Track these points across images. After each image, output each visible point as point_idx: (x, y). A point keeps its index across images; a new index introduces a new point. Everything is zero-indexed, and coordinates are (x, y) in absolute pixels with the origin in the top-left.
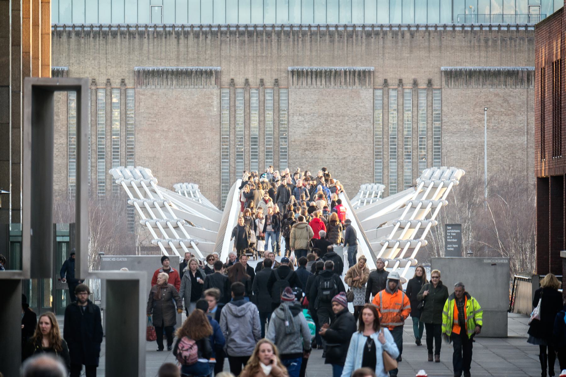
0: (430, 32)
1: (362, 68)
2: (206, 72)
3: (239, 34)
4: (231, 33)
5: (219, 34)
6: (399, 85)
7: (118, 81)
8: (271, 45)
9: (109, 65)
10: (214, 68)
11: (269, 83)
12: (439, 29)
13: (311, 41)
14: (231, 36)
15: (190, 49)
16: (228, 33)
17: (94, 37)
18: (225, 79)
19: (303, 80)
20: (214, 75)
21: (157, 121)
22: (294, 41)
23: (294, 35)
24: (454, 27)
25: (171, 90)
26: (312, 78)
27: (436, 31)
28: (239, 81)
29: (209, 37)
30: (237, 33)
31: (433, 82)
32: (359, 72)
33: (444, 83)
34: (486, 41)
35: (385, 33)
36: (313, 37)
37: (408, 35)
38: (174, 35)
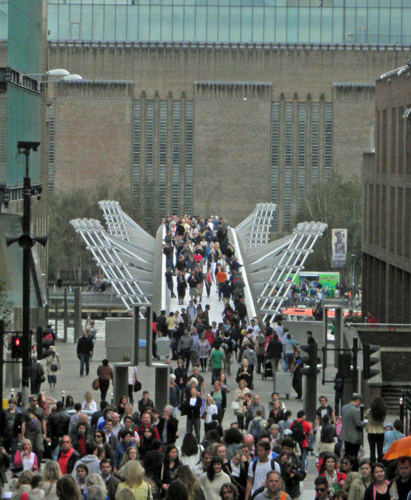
0: (323, 51)
1: (261, 83)
2: (120, 85)
4: (143, 49)
5: (132, 50)
6: (294, 99)
8: (179, 61)
10: (127, 82)
11: (177, 96)
12: (331, 48)
13: (215, 58)
18: (137, 92)
19: (208, 94)
20: (127, 88)
22: (200, 55)
23: (200, 51)
24: (345, 46)
25: (88, 100)
26: (215, 91)
27: (328, 50)
28: (150, 94)
29: (123, 52)
30: (149, 50)
31: (325, 96)
32: (259, 87)
33: (335, 97)
34: (374, 60)
35: (282, 51)
36: (217, 54)
37: (303, 54)
38: (91, 51)
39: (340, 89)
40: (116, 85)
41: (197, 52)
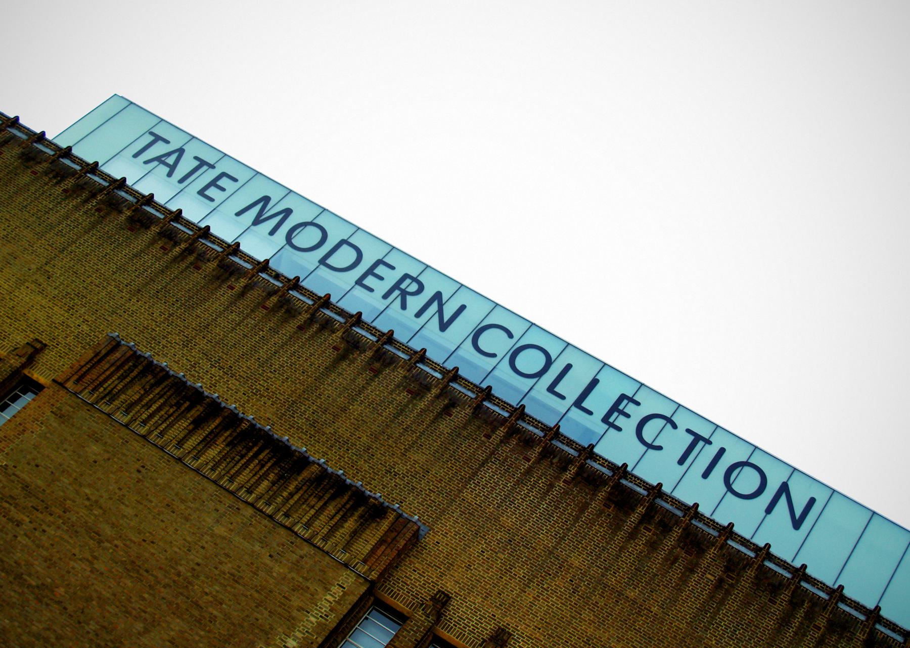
3: (577, 474)
5: (501, 432)
8: (684, 580)
9: (35, 282)
14: (545, 463)
15: (356, 409)
16: (538, 449)
20: (385, 525)
21: (27, 526)
22: (784, 621)
25: (178, 467)
30: (573, 470)
41: (785, 596)
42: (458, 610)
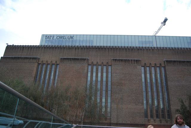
2: (84, 59)
4: (93, 48)
7: (55, 61)
13: (119, 51)
17: (49, 49)
18: (90, 62)
22: (113, 51)
23: (113, 49)
27: (160, 49)
28: (95, 63)
32: (136, 60)
34: (178, 52)
35: (144, 49)
36: (120, 50)
37: (151, 50)
39: (167, 61)
40: (82, 59)
42: (94, 62)
